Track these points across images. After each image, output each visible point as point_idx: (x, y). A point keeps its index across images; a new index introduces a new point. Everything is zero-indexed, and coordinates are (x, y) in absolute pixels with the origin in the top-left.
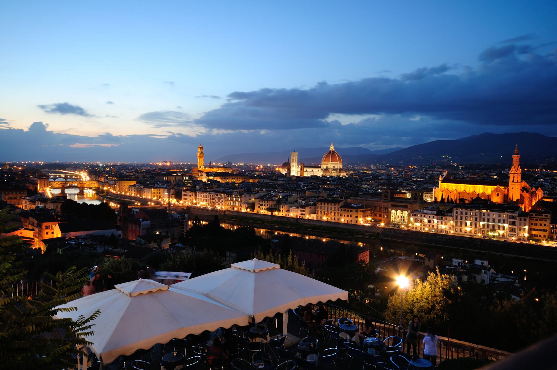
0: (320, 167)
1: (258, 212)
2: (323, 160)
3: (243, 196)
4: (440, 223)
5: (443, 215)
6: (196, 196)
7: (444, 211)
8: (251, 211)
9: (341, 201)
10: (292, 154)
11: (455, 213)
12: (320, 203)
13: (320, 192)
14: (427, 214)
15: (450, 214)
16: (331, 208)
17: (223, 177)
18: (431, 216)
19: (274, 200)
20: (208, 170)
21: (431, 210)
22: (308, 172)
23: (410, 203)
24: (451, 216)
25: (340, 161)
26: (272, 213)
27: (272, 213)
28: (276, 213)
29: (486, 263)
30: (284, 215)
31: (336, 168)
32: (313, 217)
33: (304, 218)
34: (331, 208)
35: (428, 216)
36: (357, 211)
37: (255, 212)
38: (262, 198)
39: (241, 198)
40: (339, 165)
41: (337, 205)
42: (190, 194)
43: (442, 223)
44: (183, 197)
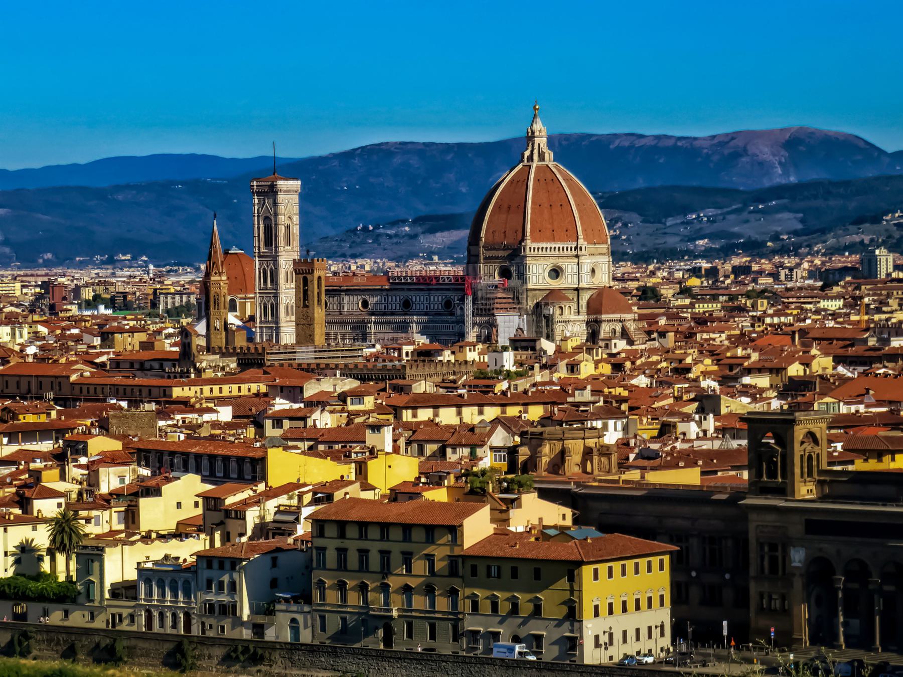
9: (474, 510)
30: (100, 623)
31: (567, 281)
33: (228, 634)
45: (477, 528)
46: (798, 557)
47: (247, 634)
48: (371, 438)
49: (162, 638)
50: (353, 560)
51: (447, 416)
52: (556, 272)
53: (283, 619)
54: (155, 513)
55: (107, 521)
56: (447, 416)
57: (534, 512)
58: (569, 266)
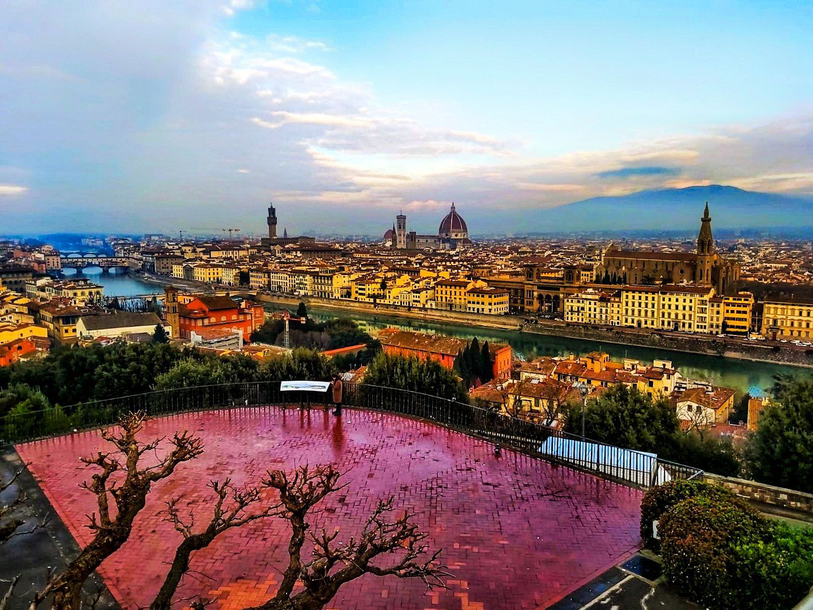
1: (356, 298)
3: (335, 277)
5: (609, 301)
7: (610, 296)
11: (624, 297)
12: (439, 286)
13: (439, 271)
15: (617, 300)
16: (455, 292)
19: (377, 283)
26: (375, 301)
27: (375, 301)
29: (669, 365)
30: (391, 303)
31: (459, 237)
32: (431, 305)
34: (455, 292)
35: (588, 302)
36: (490, 297)
38: (361, 281)
41: (463, 288)
45: (470, 287)
46: (535, 294)
47: (422, 306)
48: (439, 268)
49: (404, 307)
50: (444, 292)
51: (448, 264)
52: (456, 235)
53: (429, 303)
54: (399, 282)
55: (390, 283)
56: (448, 264)
57: (480, 284)
58: (459, 234)
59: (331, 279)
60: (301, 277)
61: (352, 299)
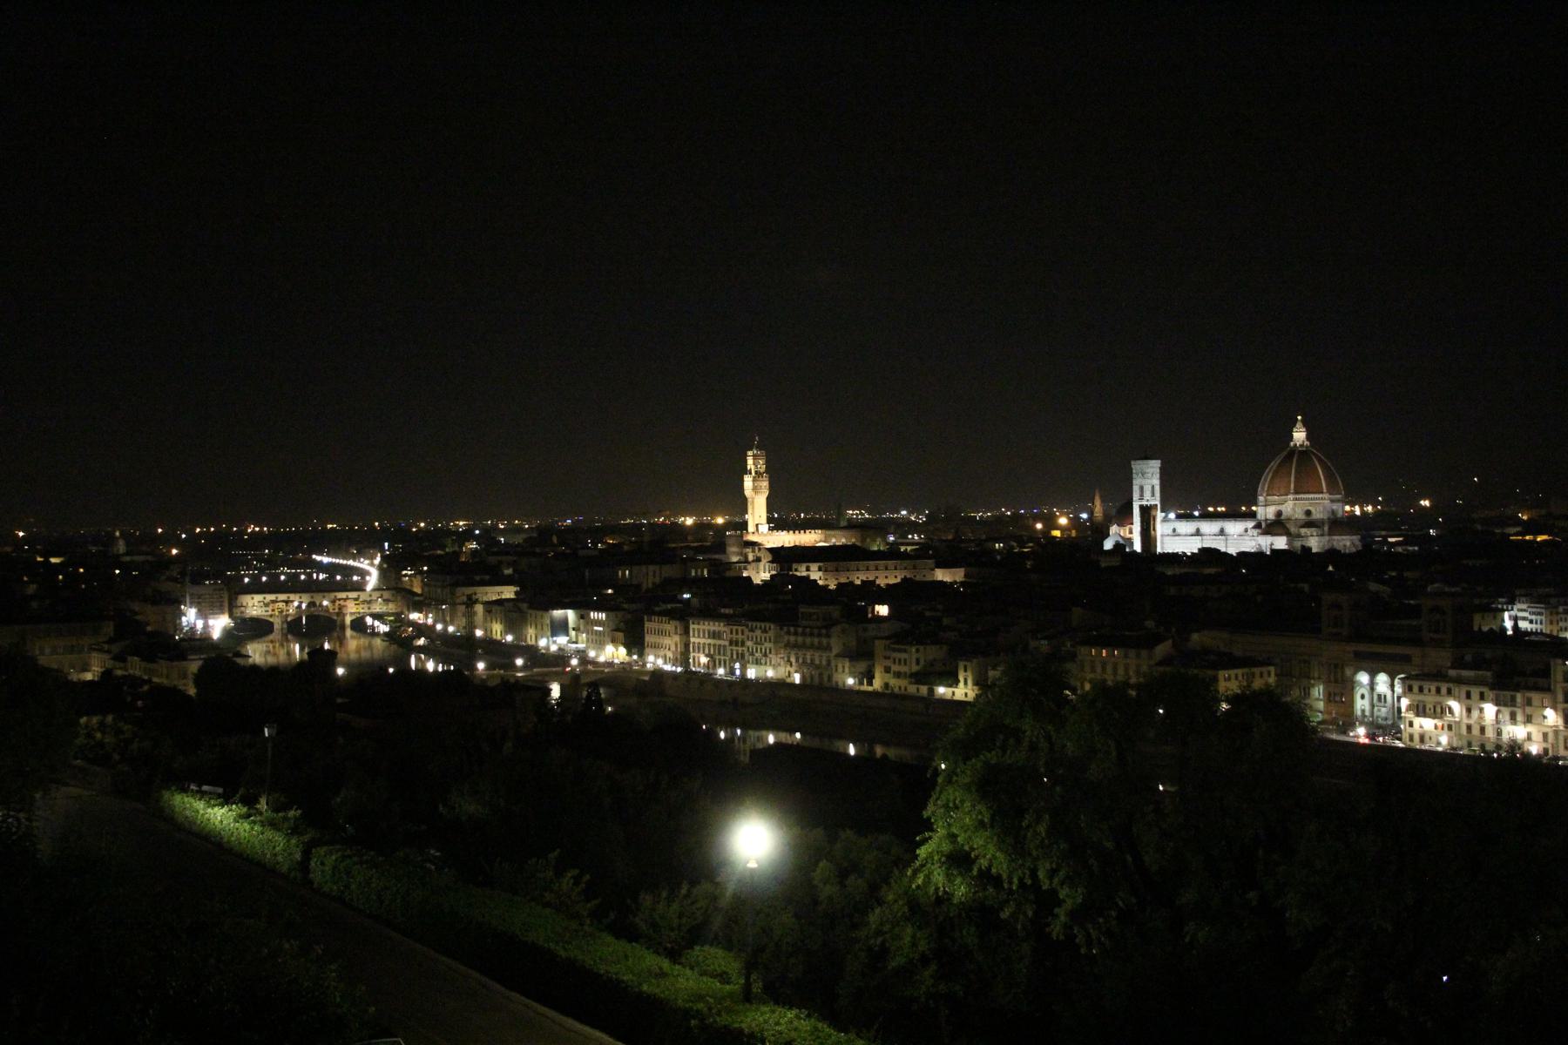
0: (1253, 515)
2: (1263, 486)
3: (836, 630)
4: (1505, 715)
5: (1517, 688)
6: (686, 632)
8: (861, 683)
10: (1137, 466)
14: (1459, 681)
15: (1541, 681)
17: (830, 565)
18: (1475, 691)
20: (786, 539)
21: (1475, 666)
22: (1179, 537)
23: (1417, 642)
24: (1547, 690)
25: (1332, 489)
26: (931, 691)
28: (941, 690)
31: (1318, 514)
35: (1464, 689)
37: (877, 684)
39: (828, 636)
40: (1321, 504)
41: (1144, 653)
42: (670, 626)
43: (1513, 718)
44: (649, 639)
59: (828, 636)
60: (758, 632)
61: (877, 684)
